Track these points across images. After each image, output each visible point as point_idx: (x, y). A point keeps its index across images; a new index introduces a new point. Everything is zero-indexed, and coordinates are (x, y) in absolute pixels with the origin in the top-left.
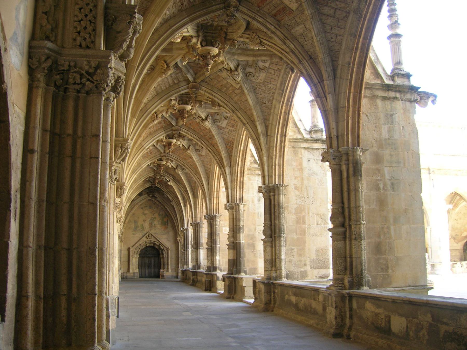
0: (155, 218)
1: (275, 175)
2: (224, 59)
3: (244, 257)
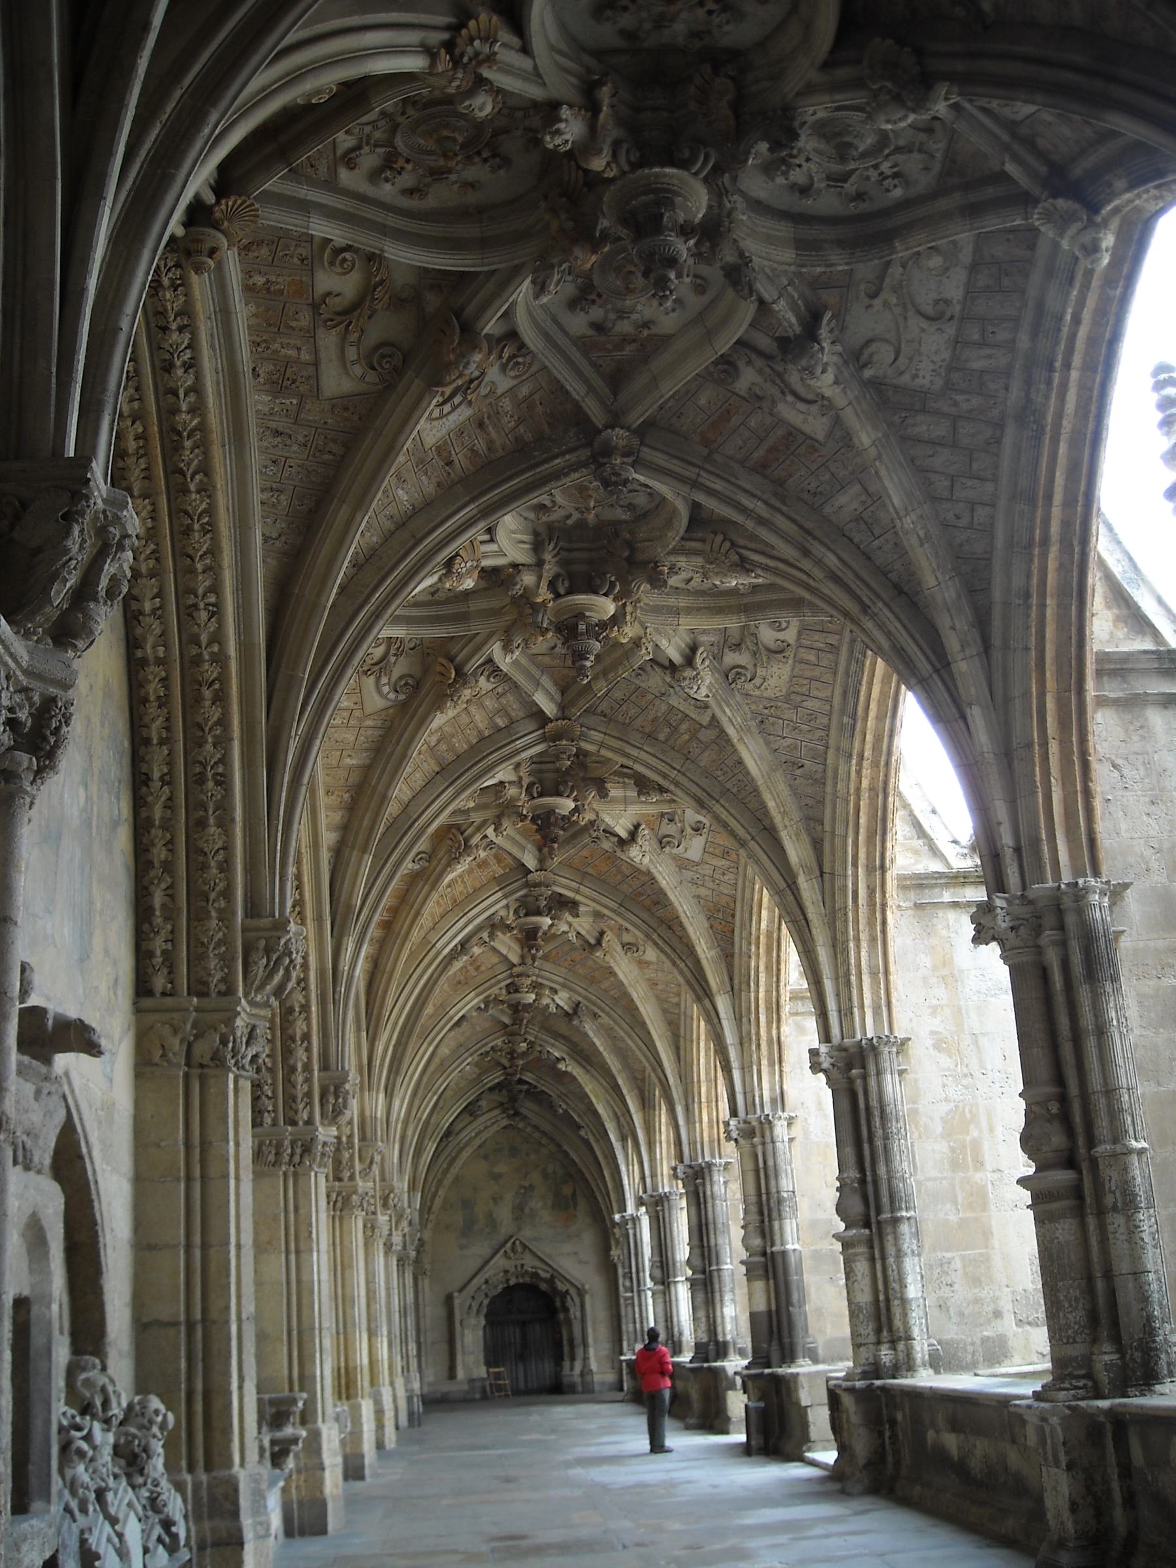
0: (532, 1187)
1: (862, 1006)
2: (642, 633)
3: (802, 1302)
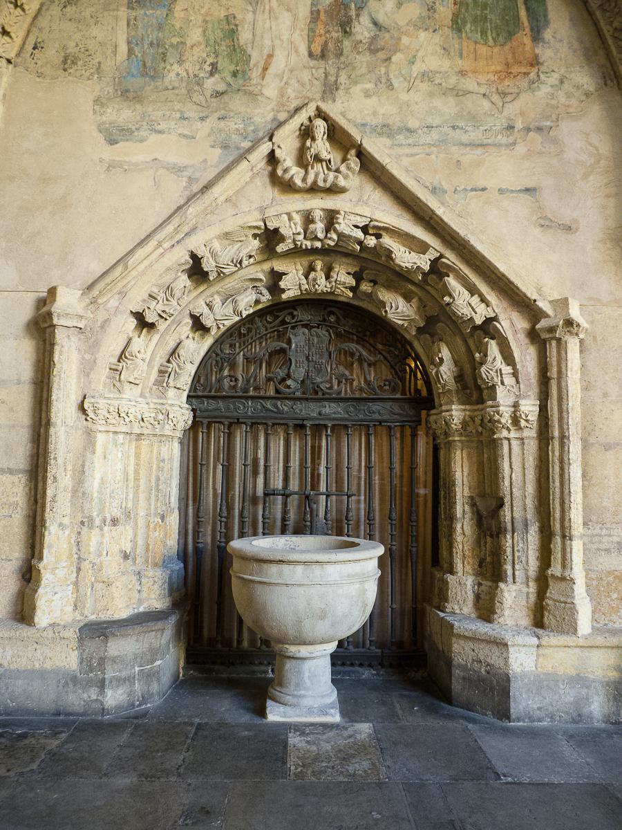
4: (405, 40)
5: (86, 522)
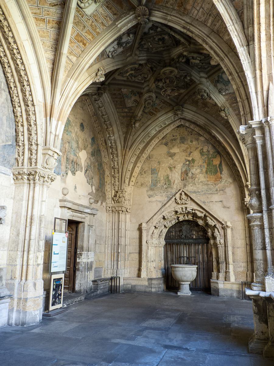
0: (193, 160)
4: (197, 176)
5: (148, 261)
